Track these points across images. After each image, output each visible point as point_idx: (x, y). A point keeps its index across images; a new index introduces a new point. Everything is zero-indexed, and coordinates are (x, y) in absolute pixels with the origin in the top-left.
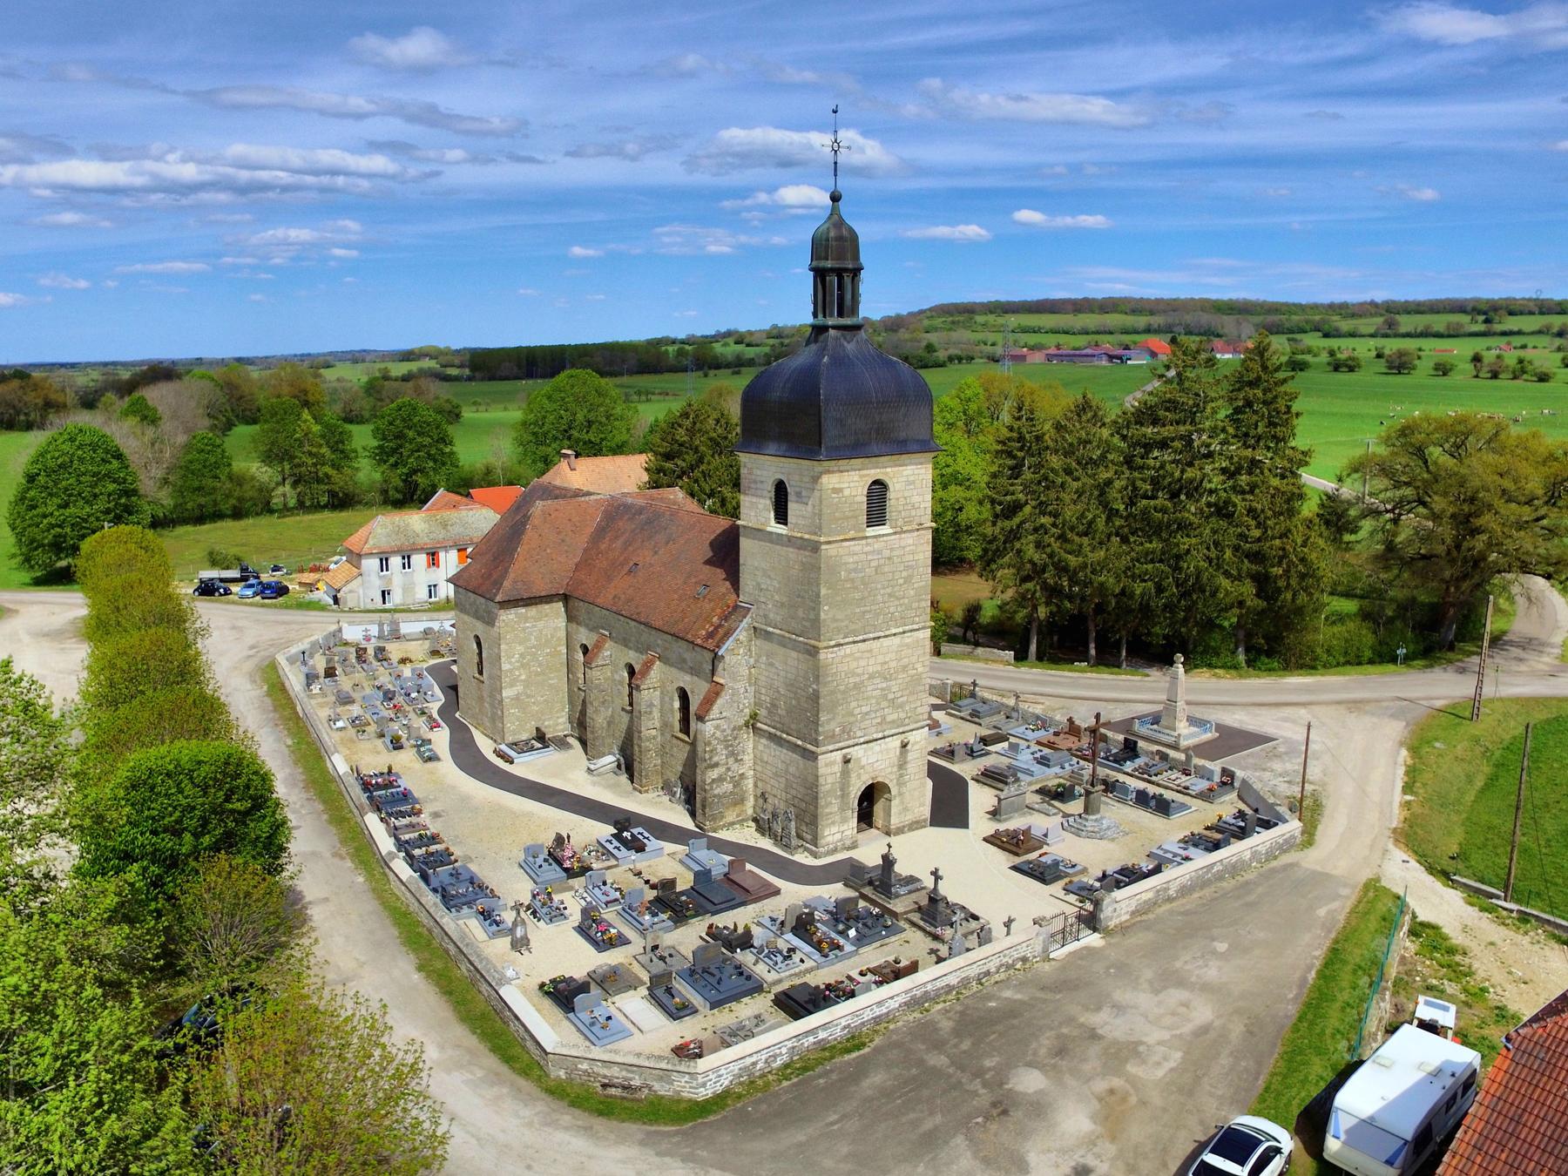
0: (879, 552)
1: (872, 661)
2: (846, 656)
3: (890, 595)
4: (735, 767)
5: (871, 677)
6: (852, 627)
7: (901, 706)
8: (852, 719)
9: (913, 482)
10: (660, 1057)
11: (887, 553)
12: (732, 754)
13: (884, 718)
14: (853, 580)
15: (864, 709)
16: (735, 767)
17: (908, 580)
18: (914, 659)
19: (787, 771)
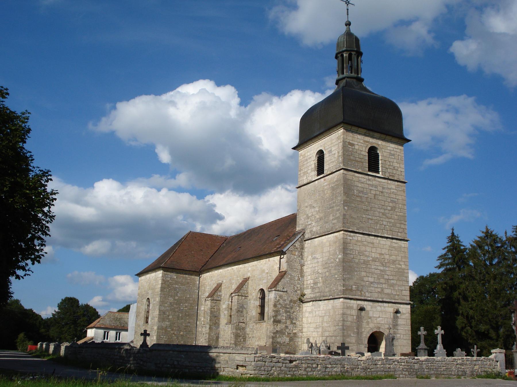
0: (376, 187)
1: (374, 250)
2: (357, 241)
3: (383, 214)
4: (291, 327)
5: (374, 260)
6: (362, 225)
7: (393, 285)
8: (363, 283)
9: (394, 155)
10: (227, 348)
11: (380, 189)
12: (289, 318)
13: (382, 289)
14: (361, 197)
15: (371, 280)
16: (291, 327)
17: (393, 209)
18: (399, 258)
19: (323, 322)
